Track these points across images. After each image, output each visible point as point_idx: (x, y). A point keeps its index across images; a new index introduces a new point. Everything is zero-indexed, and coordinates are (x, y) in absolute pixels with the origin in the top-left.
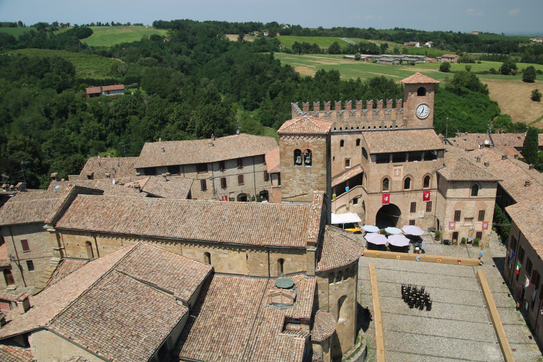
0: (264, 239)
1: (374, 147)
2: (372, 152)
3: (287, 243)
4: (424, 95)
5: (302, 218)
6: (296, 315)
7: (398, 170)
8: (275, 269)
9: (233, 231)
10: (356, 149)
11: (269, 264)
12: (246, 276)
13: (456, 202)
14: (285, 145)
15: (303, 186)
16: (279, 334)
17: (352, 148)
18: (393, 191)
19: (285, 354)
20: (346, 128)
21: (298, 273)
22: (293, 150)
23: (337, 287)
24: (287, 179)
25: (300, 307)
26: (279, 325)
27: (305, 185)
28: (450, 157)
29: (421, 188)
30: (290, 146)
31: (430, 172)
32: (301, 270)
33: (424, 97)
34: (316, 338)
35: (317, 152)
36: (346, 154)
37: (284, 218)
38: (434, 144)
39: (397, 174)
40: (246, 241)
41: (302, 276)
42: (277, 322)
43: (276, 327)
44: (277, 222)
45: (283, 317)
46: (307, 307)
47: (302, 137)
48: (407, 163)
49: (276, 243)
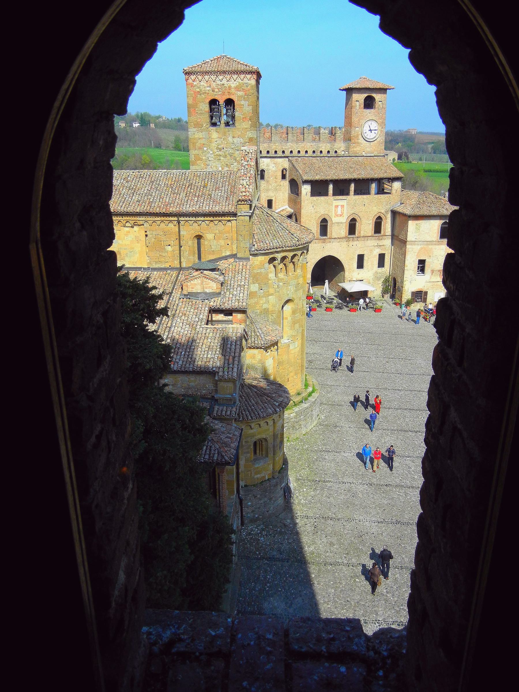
0: (172, 205)
1: (306, 173)
2: (305, 178)
3: (207, 208)
4: (372, 108)
5: (227, 183)
6: (226, 304)
7: (340, 207)
8: (189, 255)
9: (123, 200)
10: (282, 183)
11: (180, 247)
12: (144, 269)
13: (419, 247)
14: (195, 92)
15: (222, 158)
16: (203, 326)
17: (276, 182)
18: (333, 237)
19: (214, 347)
20: (268, 152)
21: (226, 258)
22: (208, 101)
23: (281, 284)
24: (200, 148)
25: (231, 296)
26: (201, 316)
27: (225, 156)
28: (408, 195)
29: (370, 235)
30: (203, 93)
31: (383, 211)
32: (228, 253)
33: (372, 110)
34: (256, 342)
35: (243, 102)
36: (268, 190)
37: (200, 184)
38: (387, 171)
39: (339, 212)
40: (145, 208)
41: (232, 260)
42: (198, 313)
43: (197, 319)
44: (189, 189)
45: (207, 309)
46: (241, 295)
47: (221, 77)
48: (352, 198)
49: (191, 209)
